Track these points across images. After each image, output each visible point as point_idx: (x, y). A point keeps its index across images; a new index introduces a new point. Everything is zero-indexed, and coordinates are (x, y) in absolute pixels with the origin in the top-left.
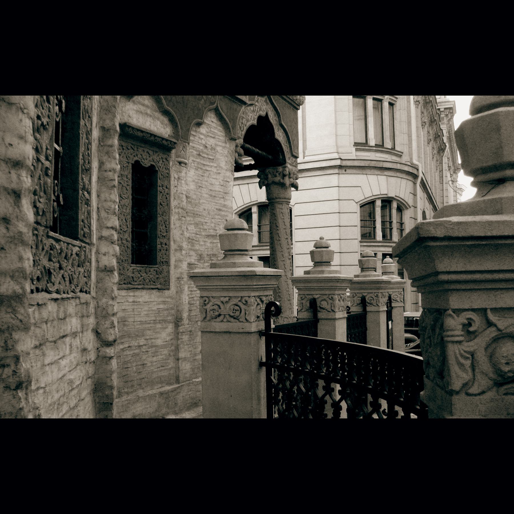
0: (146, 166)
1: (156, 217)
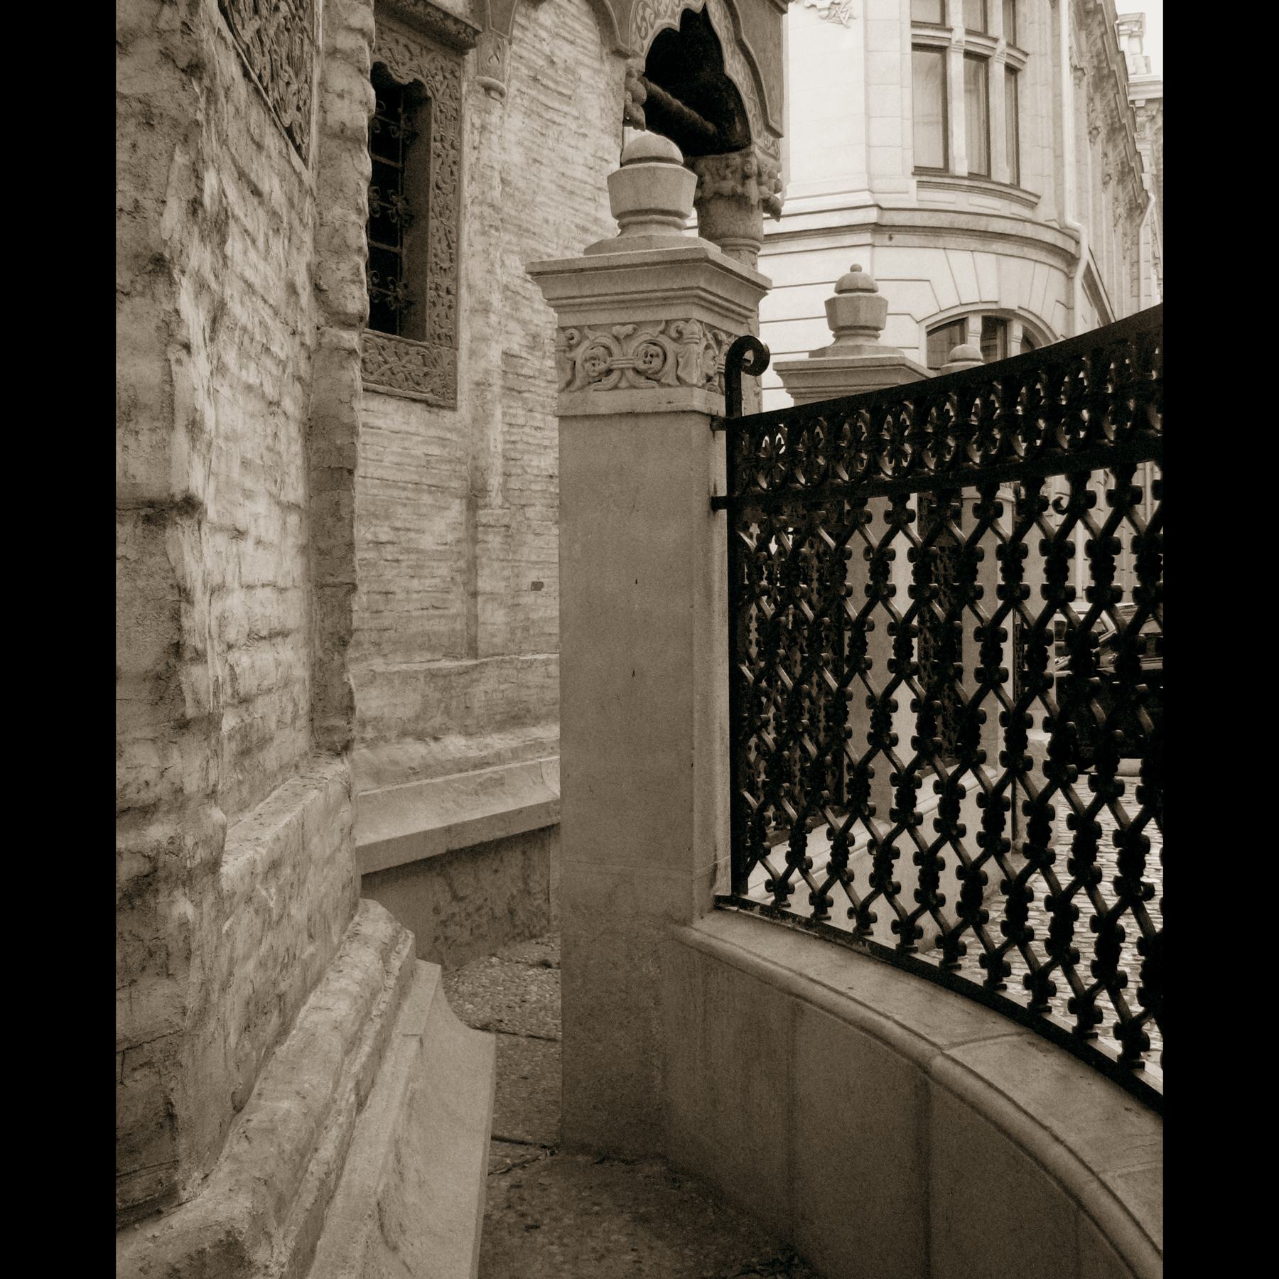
1: (426, 217)
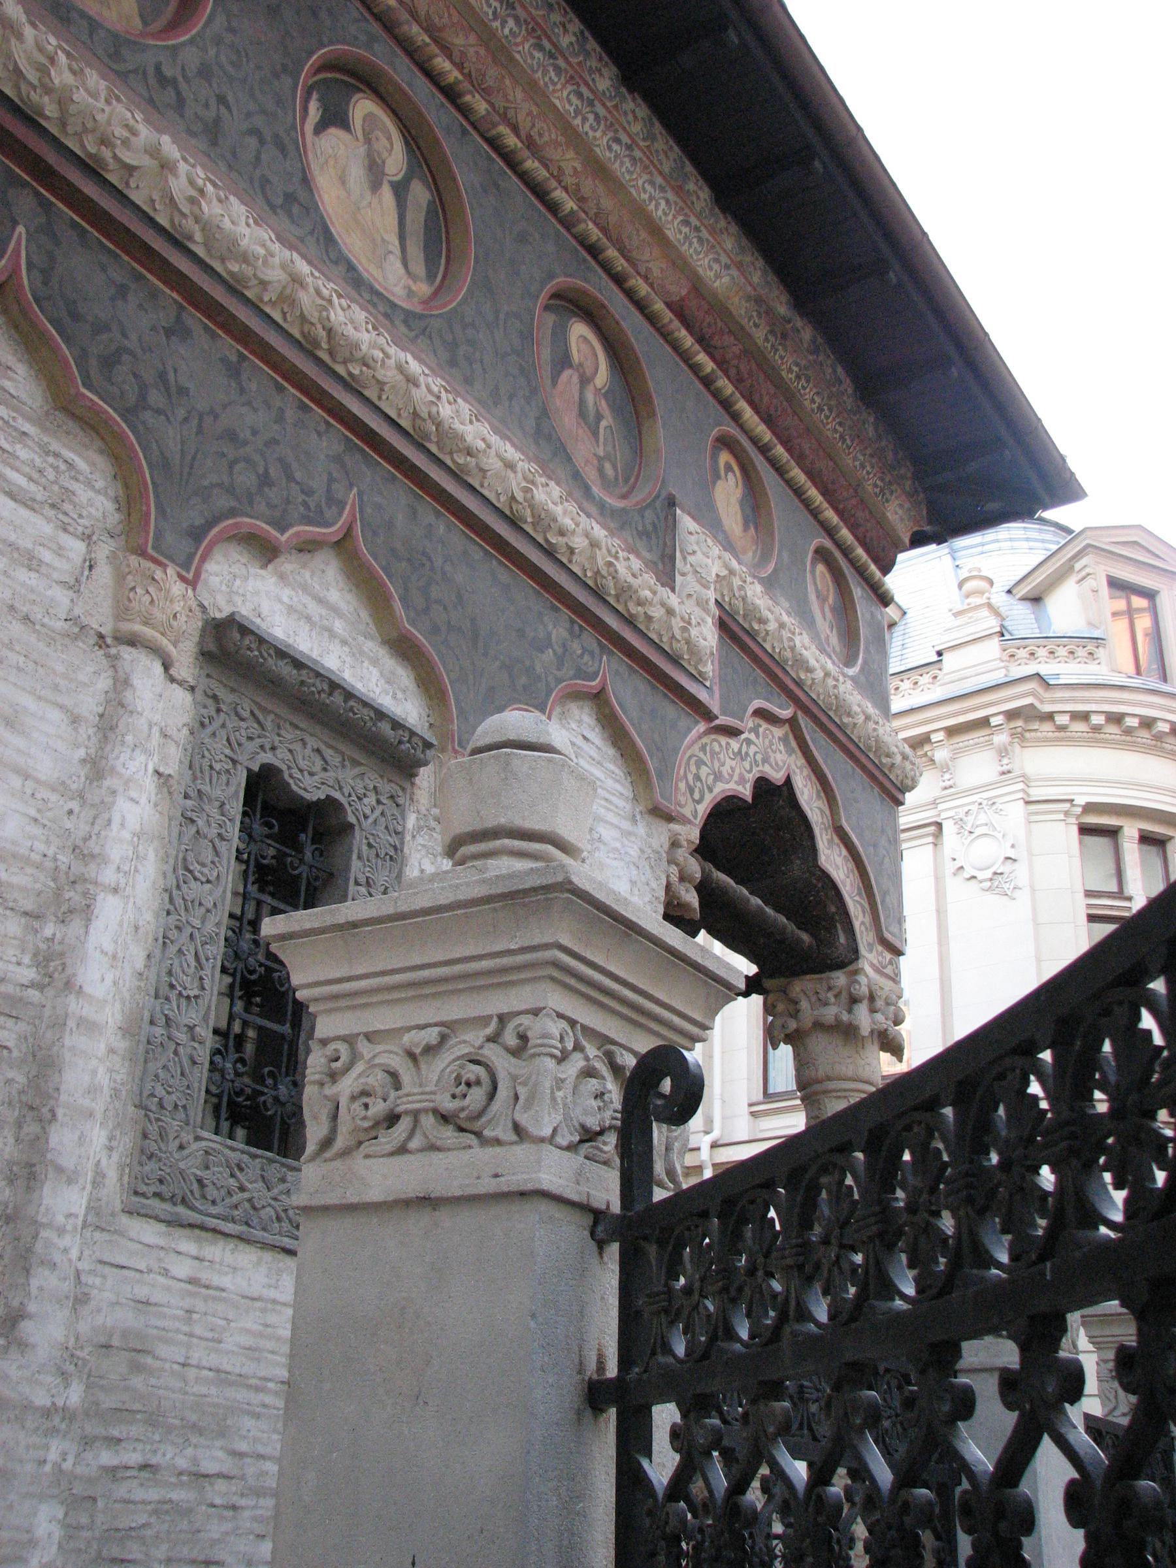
0: (307, 796)
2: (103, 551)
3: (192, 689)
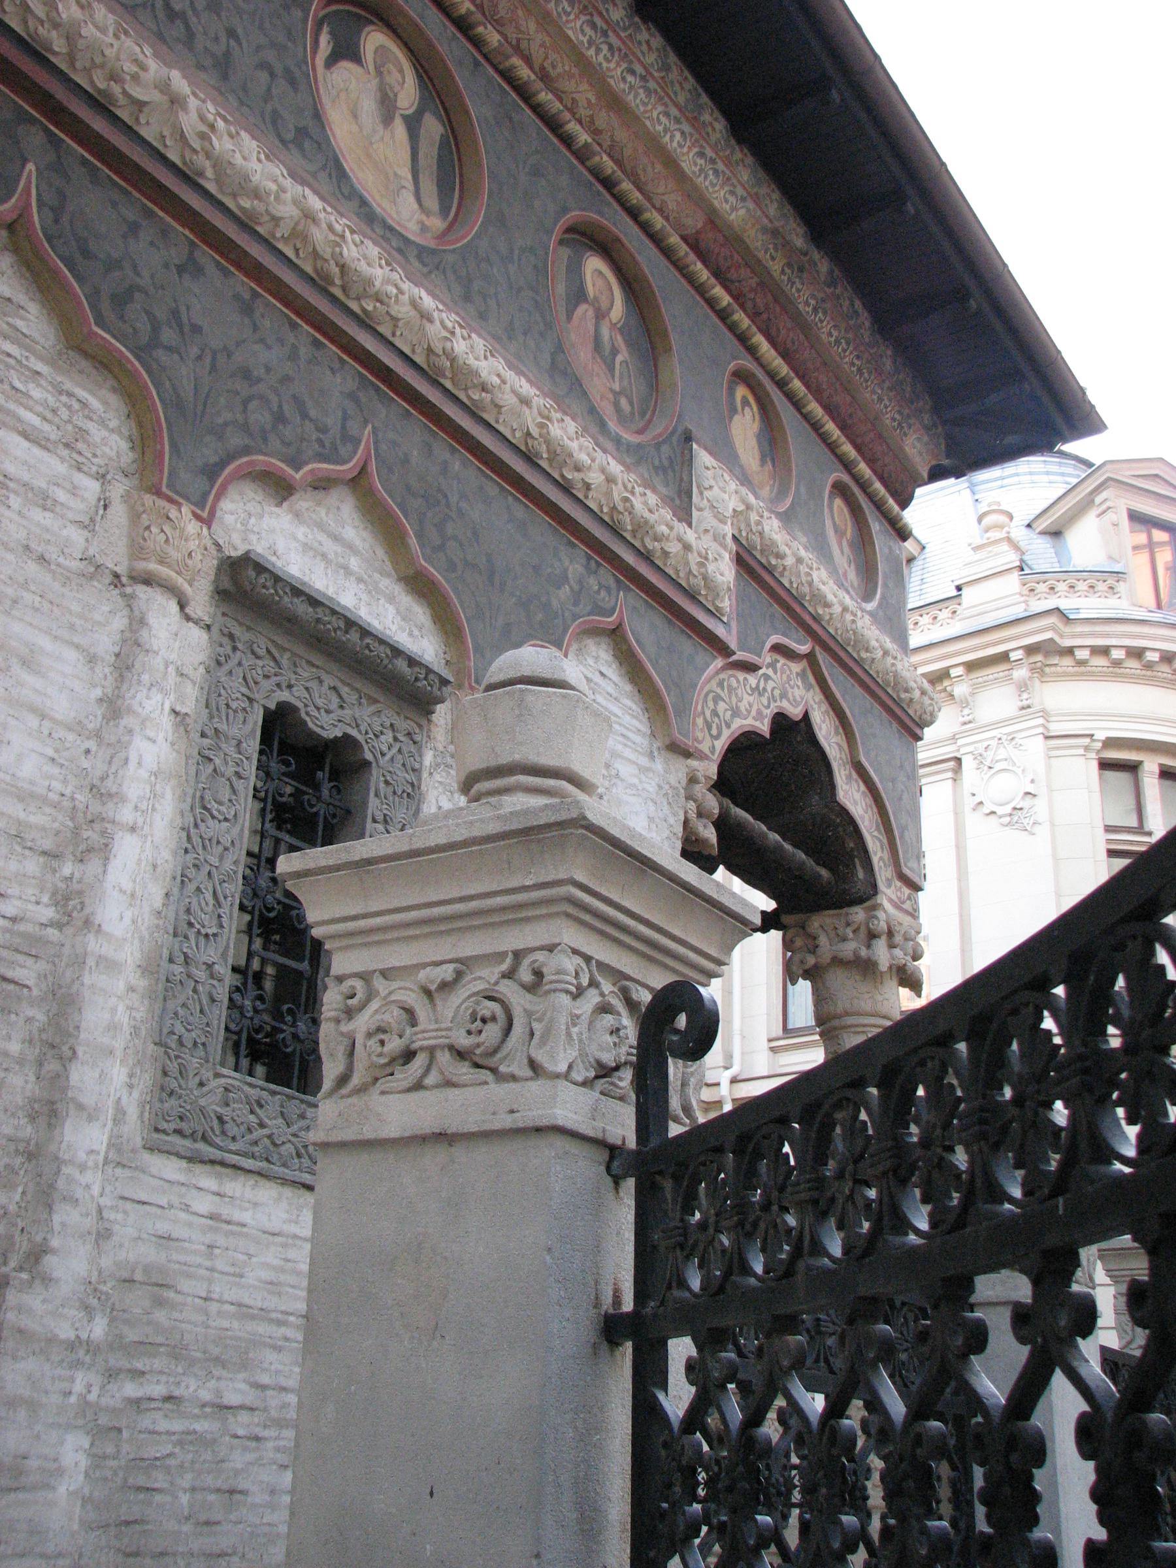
0: (324, 734)
2: (118, 489)
3: (208, 627)
